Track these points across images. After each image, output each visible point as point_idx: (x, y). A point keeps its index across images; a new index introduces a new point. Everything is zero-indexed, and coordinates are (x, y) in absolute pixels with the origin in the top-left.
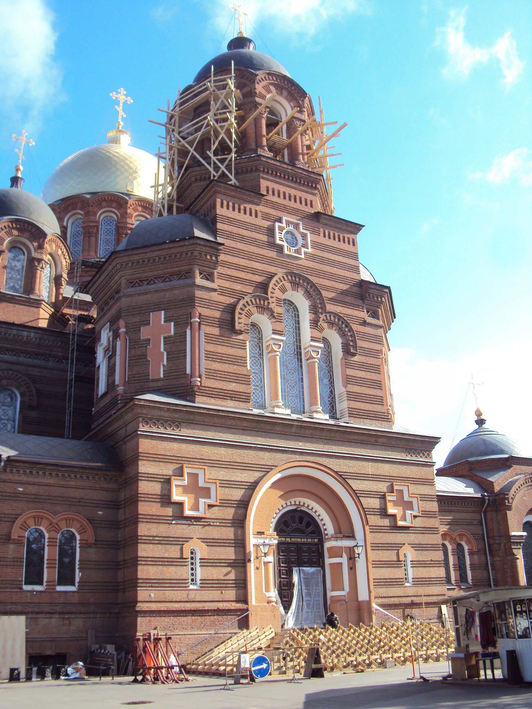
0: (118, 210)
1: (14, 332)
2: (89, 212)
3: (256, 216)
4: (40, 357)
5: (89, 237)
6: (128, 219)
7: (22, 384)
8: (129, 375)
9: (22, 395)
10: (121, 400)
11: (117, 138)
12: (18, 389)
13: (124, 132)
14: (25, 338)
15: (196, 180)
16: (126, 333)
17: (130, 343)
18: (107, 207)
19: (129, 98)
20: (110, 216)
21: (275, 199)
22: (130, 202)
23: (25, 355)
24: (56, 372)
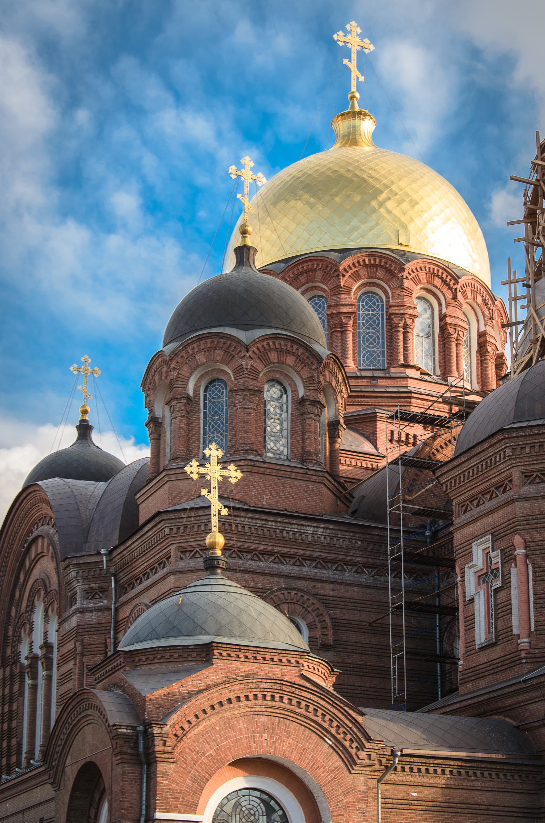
1: (295, 528)
2: (338, 287)
4: (330, 565)
5: (342, 332)
6: (406, 299)
7: (309, 609)
8: (536, 622)
10: (526, 658)
11: (354, 127)
12: (304, 618)
13: (365, 115)
14: (310, 536)
16: (527, 556)
17: (534, 572)
19: (367, 41)
20: (372, 293)
22: (409, 266)
23: (308, 562)
24: (356, 589)
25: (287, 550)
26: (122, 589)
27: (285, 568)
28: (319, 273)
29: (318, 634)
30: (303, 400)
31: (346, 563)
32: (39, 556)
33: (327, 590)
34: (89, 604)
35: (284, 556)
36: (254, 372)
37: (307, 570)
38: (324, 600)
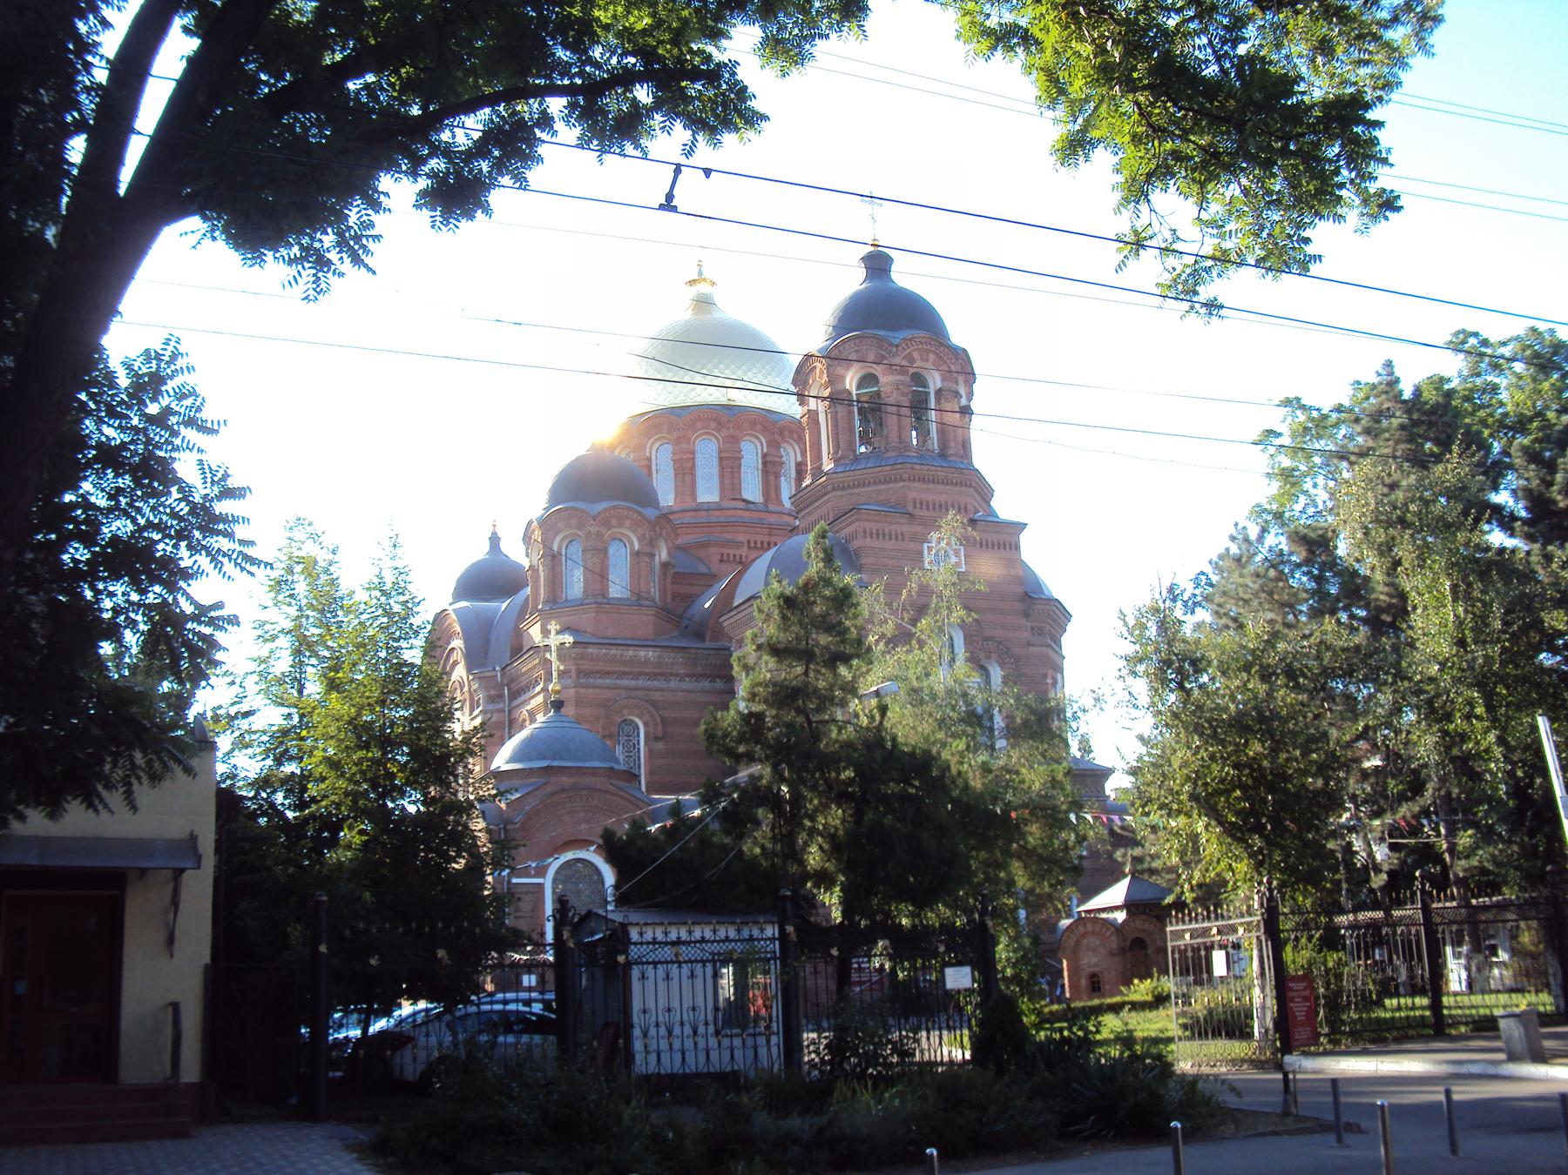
0: (719, 431)
3: (903, 540)
9: (645, 725)
15: (834, 489)
18: (703, 428)
21: (924, 513)
25: (626, 669)
26: (515, 695)
27: (625, 682)
28: (666, 427)
29: (651, 730)
30: (638, 553)
31: (671, 675)
32: (456, 663)
33: (657, 696)
34: (490, 707)
35: (624, 673)
36: (599, 535)
37: (641, 682)
38: (654, 704)
